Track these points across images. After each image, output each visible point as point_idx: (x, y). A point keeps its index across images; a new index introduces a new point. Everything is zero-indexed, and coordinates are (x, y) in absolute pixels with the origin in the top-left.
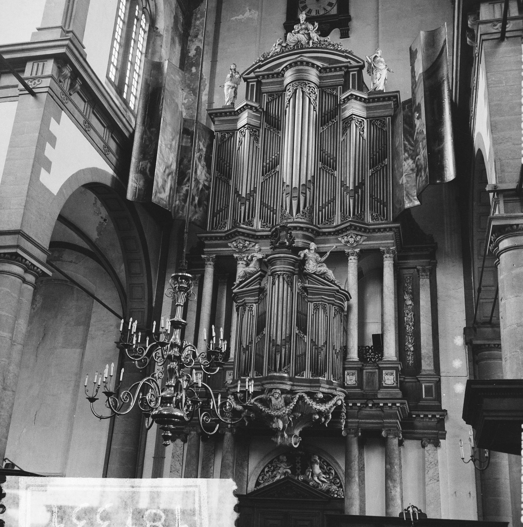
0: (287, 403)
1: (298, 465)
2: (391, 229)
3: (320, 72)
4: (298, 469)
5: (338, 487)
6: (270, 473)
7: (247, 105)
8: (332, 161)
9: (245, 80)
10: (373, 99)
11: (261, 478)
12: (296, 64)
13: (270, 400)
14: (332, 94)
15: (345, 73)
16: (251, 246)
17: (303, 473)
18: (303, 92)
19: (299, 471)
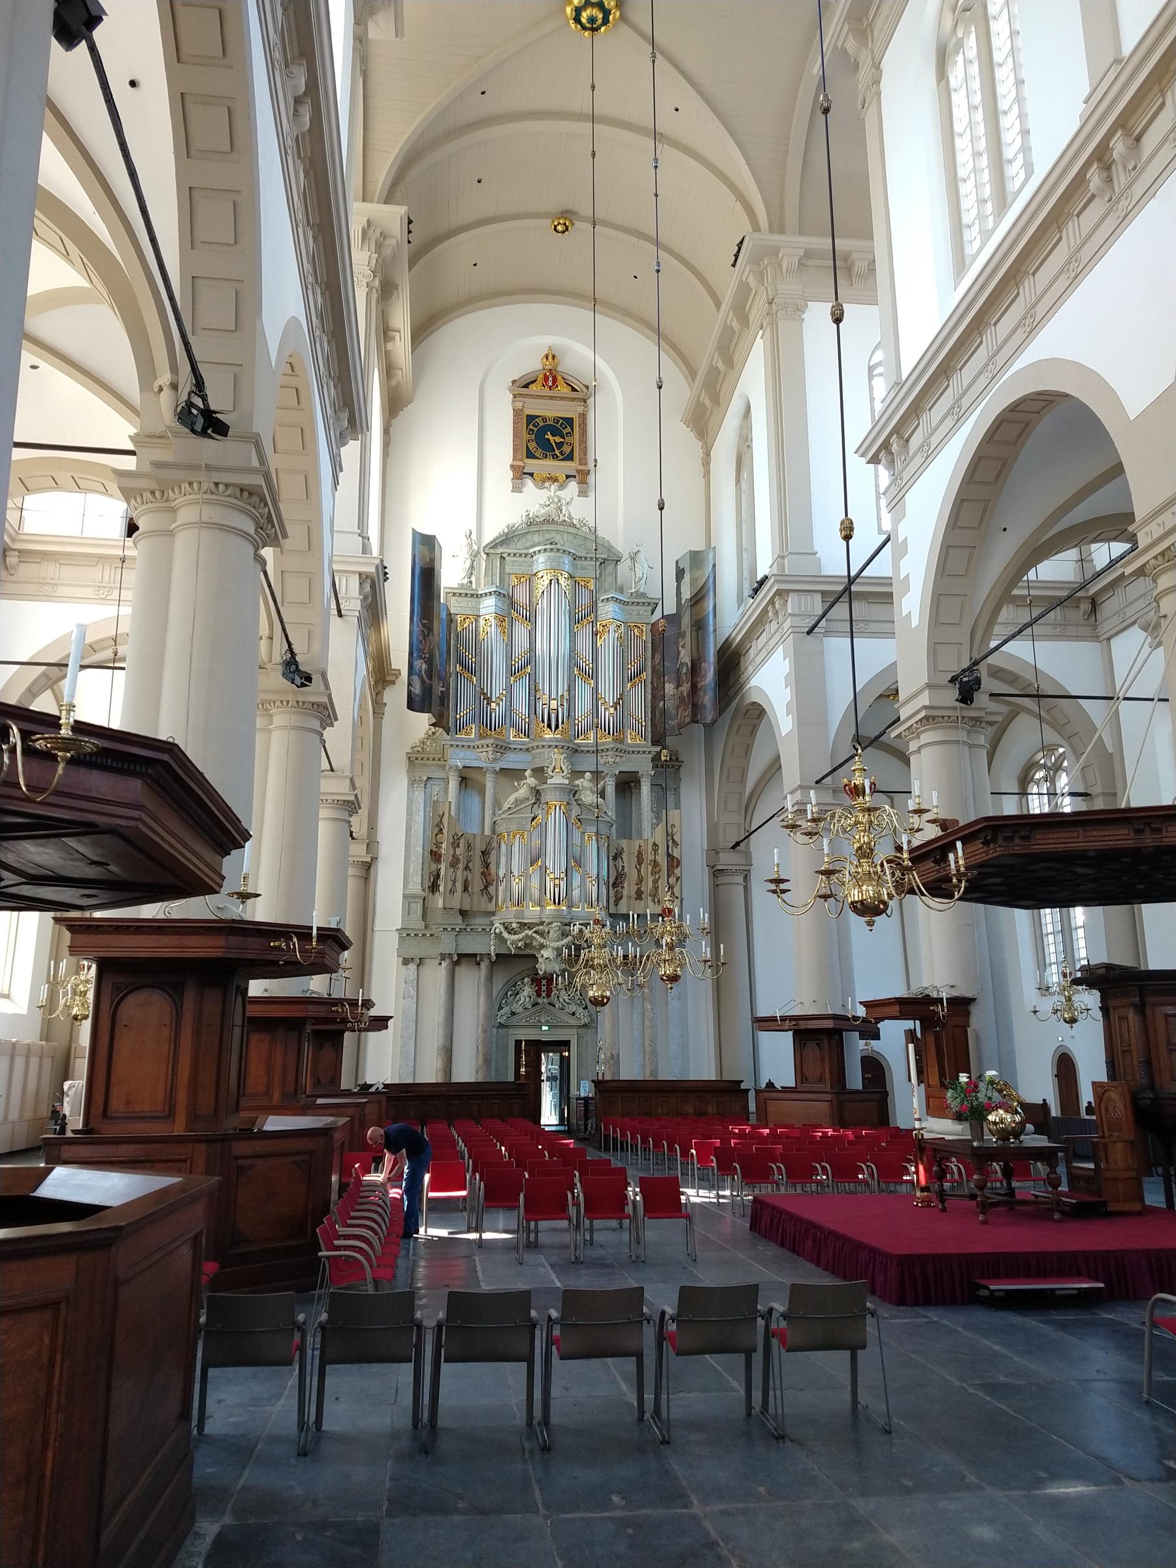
0: (565, 934)
1: (544, 988)
2: (650, 752)
3: (575, 559)
4: (544, 991)
5: (584, 1009)
6: (512, 998)
7: (495, 592)
8: (587, 667)
9: (488, 554)
10: (633, 603)
11: (504, 1001)
12: (552, 550)
13: (549, 932)
14: (586, 587)
15: (601, 563)
16: (502, 758)
17: (549, 995)
18: (558, 583)
19: (544, 994)
